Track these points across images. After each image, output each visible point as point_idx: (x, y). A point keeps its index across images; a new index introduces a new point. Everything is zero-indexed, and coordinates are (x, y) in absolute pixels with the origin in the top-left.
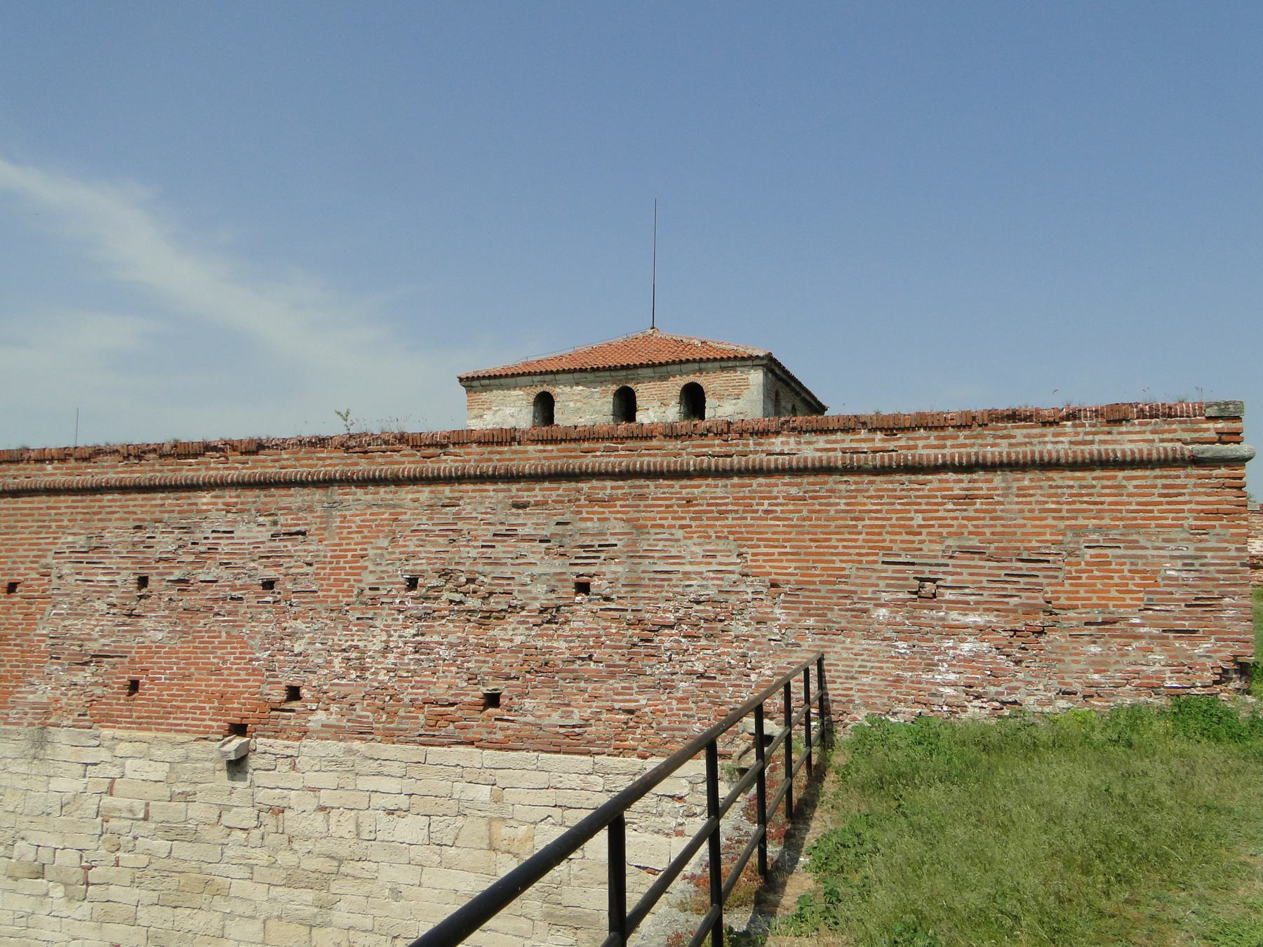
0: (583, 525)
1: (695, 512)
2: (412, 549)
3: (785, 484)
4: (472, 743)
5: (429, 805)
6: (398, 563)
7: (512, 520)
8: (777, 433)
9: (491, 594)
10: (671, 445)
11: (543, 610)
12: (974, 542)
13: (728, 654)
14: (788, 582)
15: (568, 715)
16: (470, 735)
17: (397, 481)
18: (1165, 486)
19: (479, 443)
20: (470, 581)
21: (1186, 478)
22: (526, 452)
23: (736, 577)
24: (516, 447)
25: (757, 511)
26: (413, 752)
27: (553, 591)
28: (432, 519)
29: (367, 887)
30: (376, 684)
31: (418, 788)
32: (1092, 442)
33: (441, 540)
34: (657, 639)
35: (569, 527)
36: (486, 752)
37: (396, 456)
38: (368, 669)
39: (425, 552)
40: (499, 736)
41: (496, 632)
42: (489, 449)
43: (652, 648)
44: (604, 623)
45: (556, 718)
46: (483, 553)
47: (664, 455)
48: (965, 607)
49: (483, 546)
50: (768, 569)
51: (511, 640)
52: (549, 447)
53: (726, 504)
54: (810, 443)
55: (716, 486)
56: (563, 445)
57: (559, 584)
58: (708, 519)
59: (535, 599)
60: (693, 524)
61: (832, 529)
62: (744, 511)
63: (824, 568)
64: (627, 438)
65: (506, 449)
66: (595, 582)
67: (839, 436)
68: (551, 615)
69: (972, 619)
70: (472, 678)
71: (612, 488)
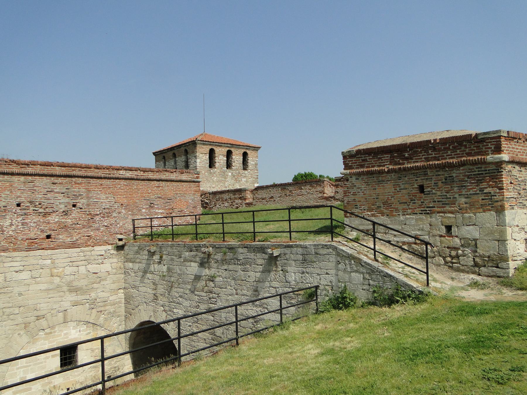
0: (73, 189)
1: (103, 187)
2: (19, 195)
3: (123, 182)
4: (43, 249)
5: (31, 267)
6: (14, 199)
7: (53, 187)
8: (121, 170)
9: (47, 208)
10: (96, 170)
11: (64, 212)
12: (160, 196)
13: (112, 221)
14: (125, 204)
15: (72, 238)
16: (43, 247)
17: (12, 174)
18: (189, 186)
19: (41, 165)
20: (40, 204)
21: (192, 184)
22: (56, 169)
23: (113, 203)
24: (52, 167)
25: (117, 188)
26: (24, 254)
27: (66, 207)
28: (25, 186)
29: (9, 295)
30: (9, 235)
31: (26, 263)
32: (178, 177)
33: (29, 192)
34: (95, 218)
35: (70, 190)
36: (48, 251)
37: (11, 166)
38: (5, 231)
39: (24, 196)
40: (52, 246)
41: (49, 218)
42: (44, 167)
43: (94, 220)
44: (81, 215)
45: (69, 239)
46: (44, 196)
47: (95, 173)
48: (159, 209)
49: (43, 195)
50: (120, 201)
51: (54, 220)
52: (63, 168)
53: (110, 186)
54: (128, 173)
55: (108, 181)
56: (67, 168)
57: (68, 205)
58: (106, 189)
59: (61, 209)
60: (103, 190)
61: (134, 192)
62: (115, 188)
63: (132, 201)
64: (85, 168)
65: (49, 167)
66: (78, 204)
67: (134, 172)
68: (66, 213)
69: (160, 211)
70: (42, 231)
71: (81, 180)
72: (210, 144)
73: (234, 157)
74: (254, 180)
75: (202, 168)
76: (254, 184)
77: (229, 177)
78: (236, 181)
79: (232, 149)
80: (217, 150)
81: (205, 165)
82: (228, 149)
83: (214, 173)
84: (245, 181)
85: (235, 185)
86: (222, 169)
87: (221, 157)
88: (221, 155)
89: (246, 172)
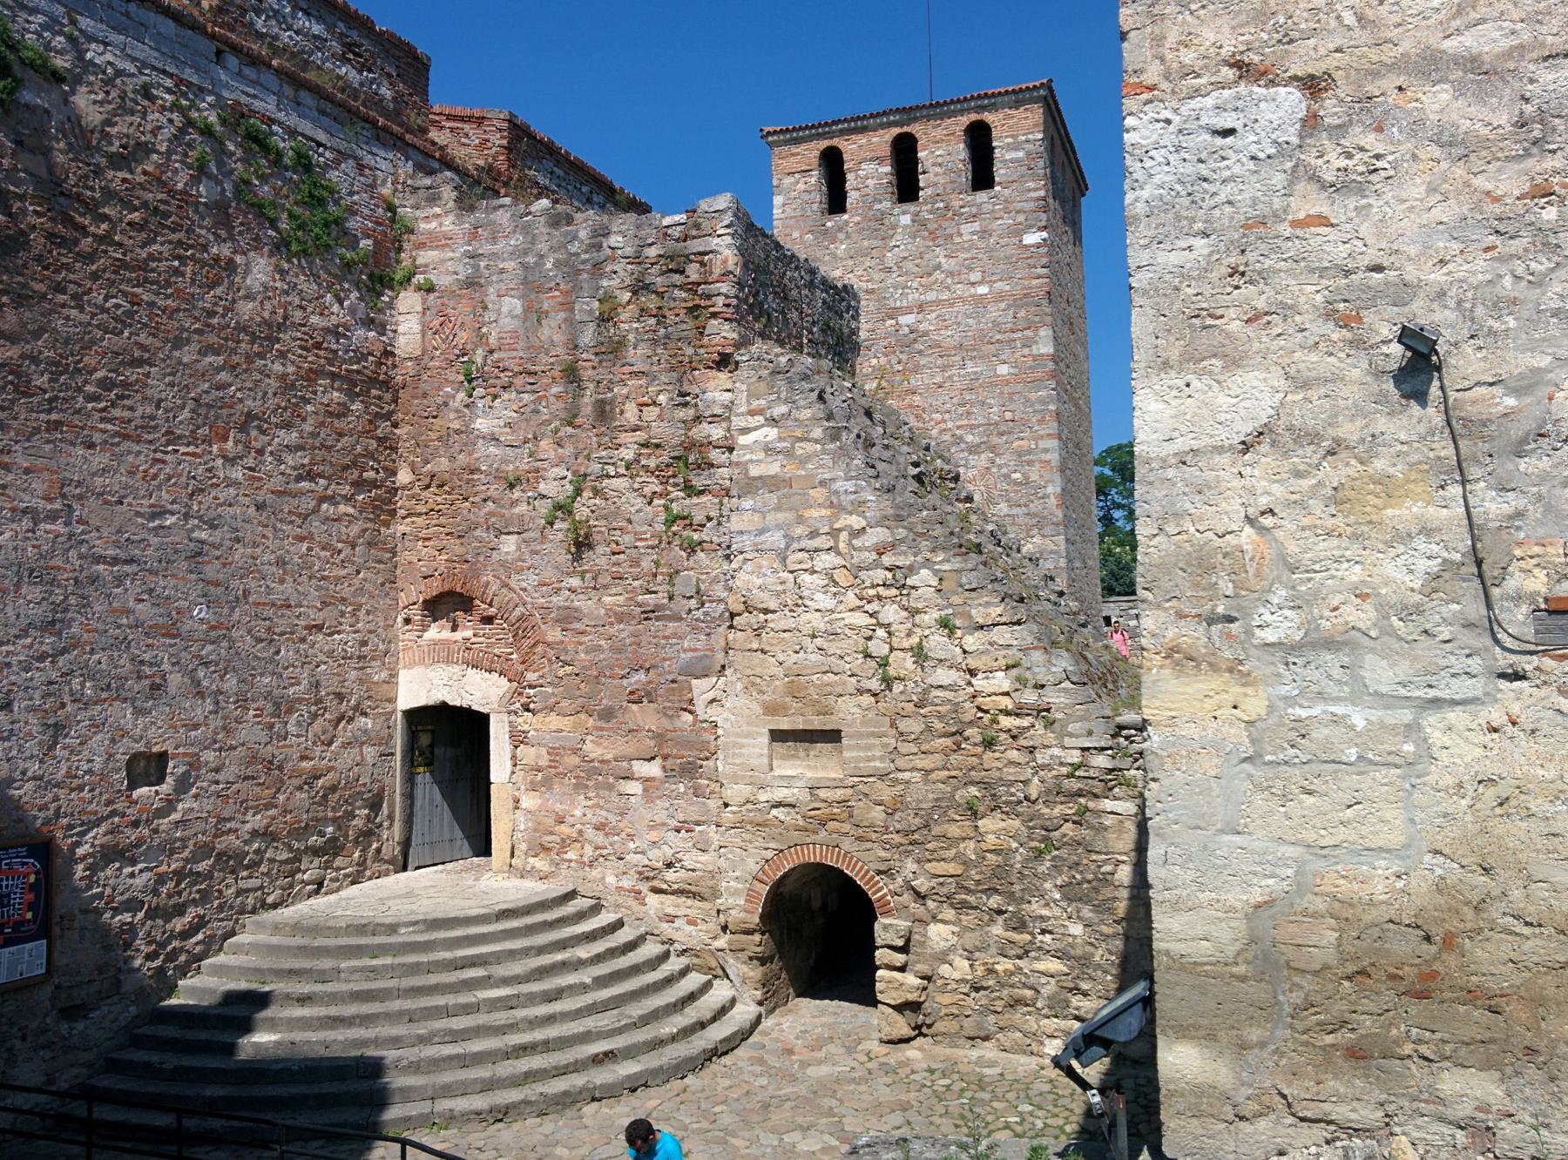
72: (818, 134)
73: (921, 155)
74: (1021, 218)
75: (792, 222)
77: (900, 230)
78: (933, 240)
79: (915, 129)
80: (851, 147)
81: (803, 209)
82: (896, 131)
83: (840, 229)
84: (973, 233)
85: (927, 256)
86: (870, 208)
87: (868, 168)
88: (865, 160)
89: (982, 196)
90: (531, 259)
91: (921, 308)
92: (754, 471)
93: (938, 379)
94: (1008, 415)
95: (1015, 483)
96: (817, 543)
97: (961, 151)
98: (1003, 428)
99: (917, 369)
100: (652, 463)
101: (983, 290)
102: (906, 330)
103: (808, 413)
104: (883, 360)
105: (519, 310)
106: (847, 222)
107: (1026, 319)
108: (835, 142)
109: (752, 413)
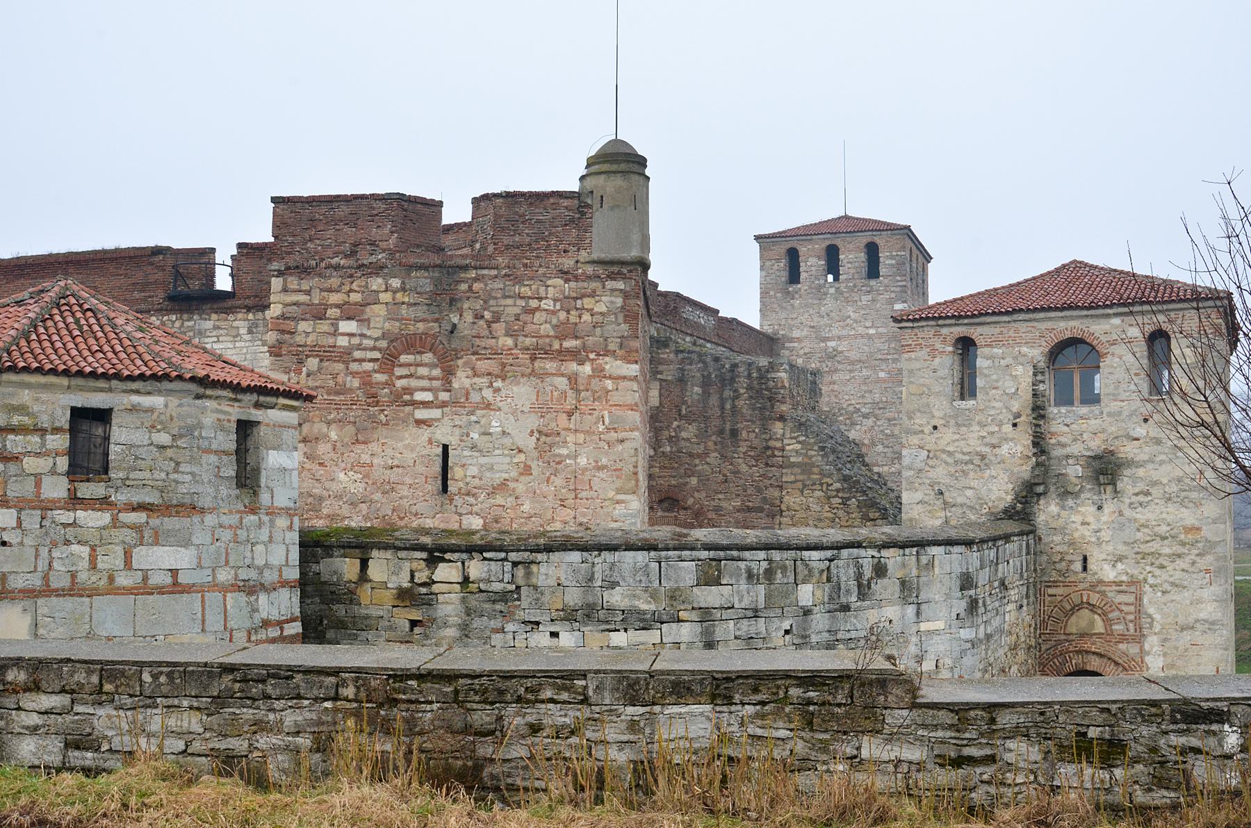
74: (893, 295)
76: (892, 304)
79: (838, 242)
80: (802, 250)
82: (828, 243)
83: (796, 292)
89: (873, 282)
90: (706, 373)
91: (839, 338)
92: (792, 460)
93: (848, 377)
94: (884, 399)
95: (887, 435)
96: (814, 487)
97: (862, 256)
98: (881, 406)
99: (836, 371)
100: (752, 454)
101: (872, 331)
102: (831, 350)
103: (812, 441)
104: (818, 364)
105: (700, 392)
106: (800, 289)
107: (894, 349)
108: (794, 245)
109: (791, 438)
